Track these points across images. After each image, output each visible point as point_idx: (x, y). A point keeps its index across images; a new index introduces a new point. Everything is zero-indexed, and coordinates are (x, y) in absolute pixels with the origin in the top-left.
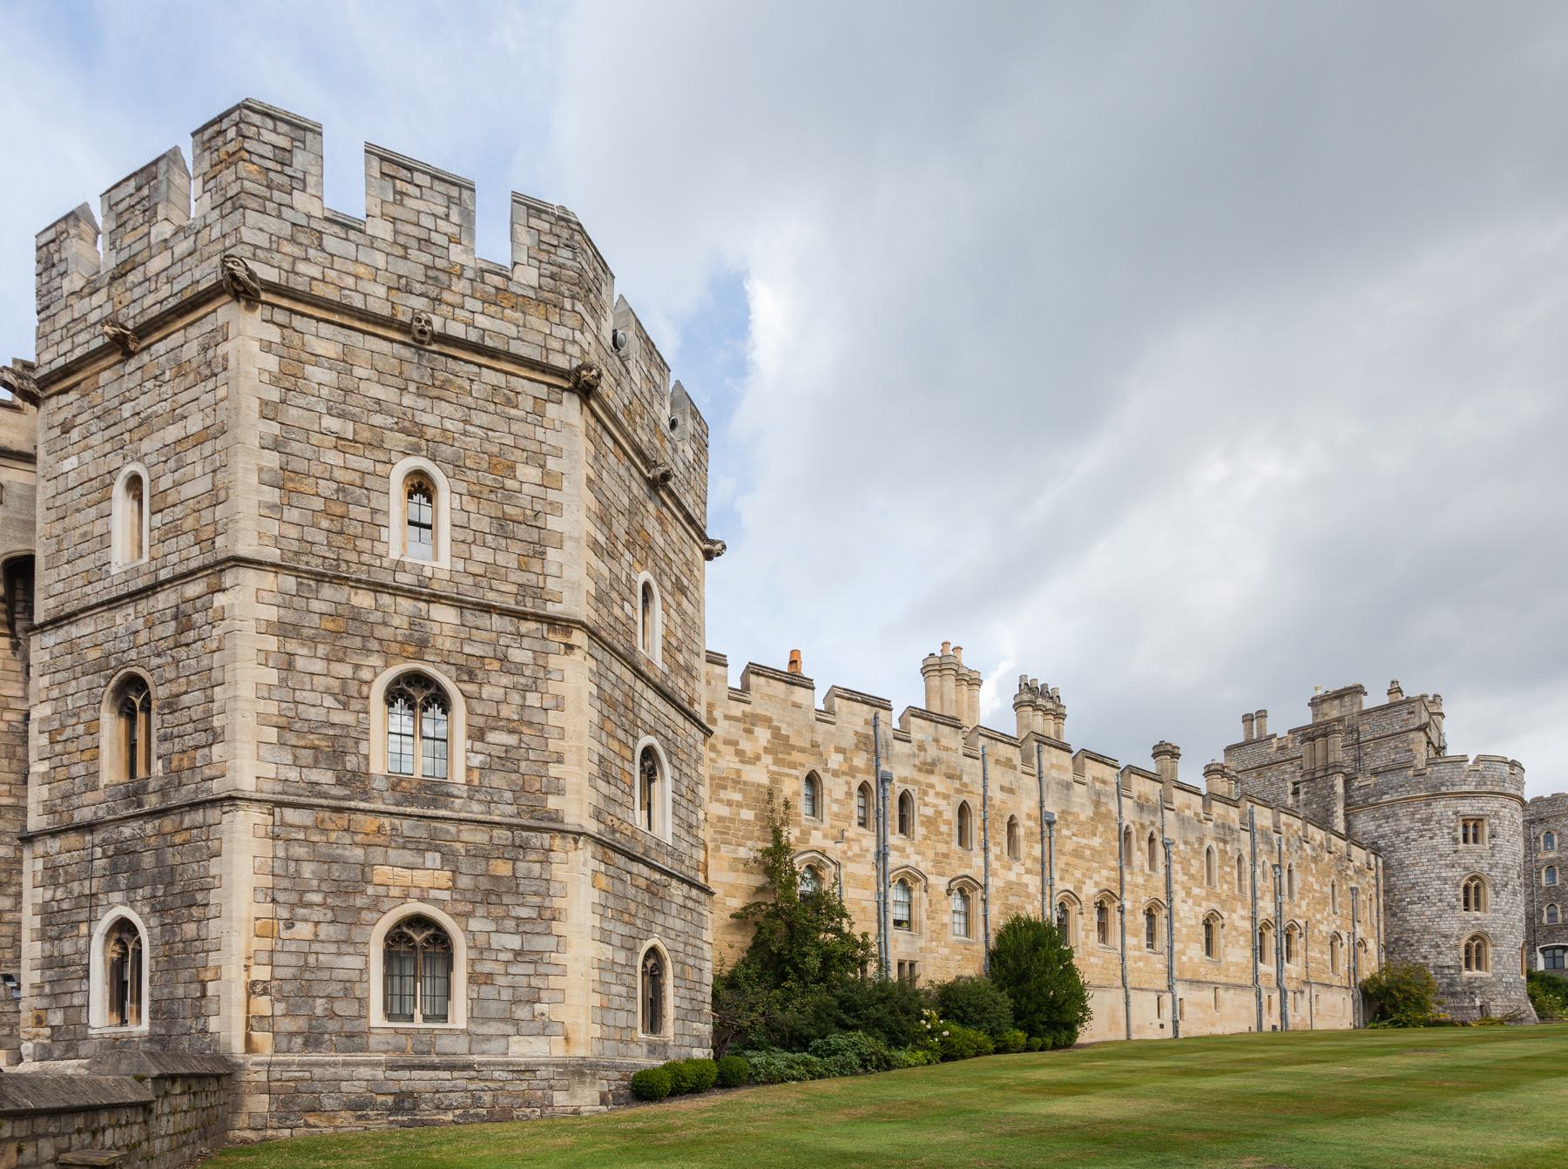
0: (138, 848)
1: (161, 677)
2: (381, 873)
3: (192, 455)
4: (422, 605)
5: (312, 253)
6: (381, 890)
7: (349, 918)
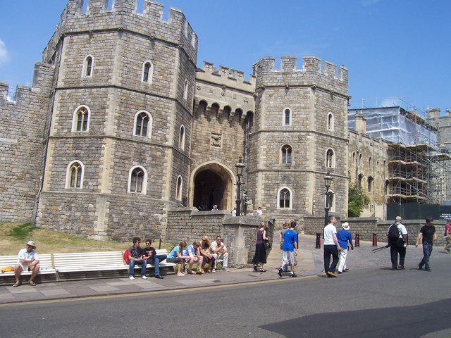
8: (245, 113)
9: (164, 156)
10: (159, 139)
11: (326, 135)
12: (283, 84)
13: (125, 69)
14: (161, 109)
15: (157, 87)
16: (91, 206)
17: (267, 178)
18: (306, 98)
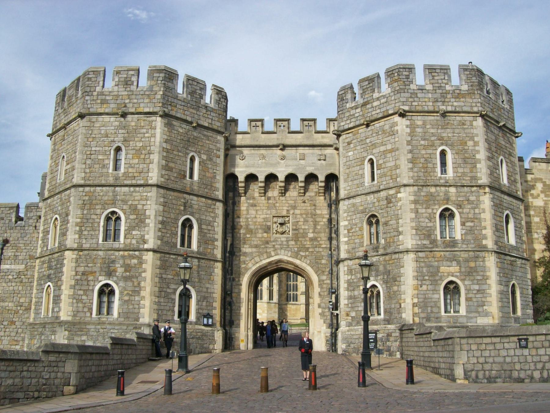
0: (378, 265)
1: (383, 216)
2: (442, 269)
3: (389, 155)
4: (447, 188)
5: (415, 99)
6: (442, 274)
7: (435, 283)
8: (322, 178)
9: (141, 263)
10: (134, 242)
11: (436, 186)
12: (362, 121)
13: (89, 162)
14: (136, 203)
15: (130, 175)
16: (53, 337)
17: (350, 271)
18: (393, 133)
